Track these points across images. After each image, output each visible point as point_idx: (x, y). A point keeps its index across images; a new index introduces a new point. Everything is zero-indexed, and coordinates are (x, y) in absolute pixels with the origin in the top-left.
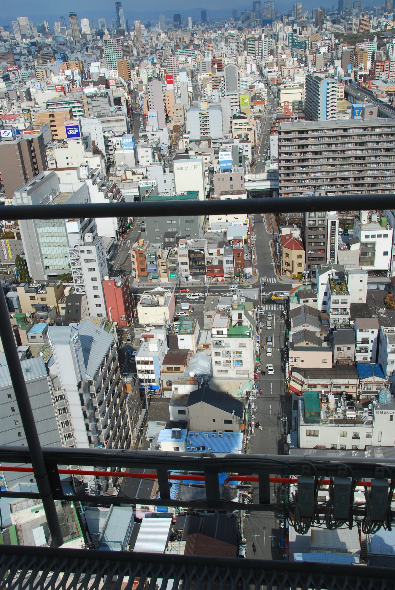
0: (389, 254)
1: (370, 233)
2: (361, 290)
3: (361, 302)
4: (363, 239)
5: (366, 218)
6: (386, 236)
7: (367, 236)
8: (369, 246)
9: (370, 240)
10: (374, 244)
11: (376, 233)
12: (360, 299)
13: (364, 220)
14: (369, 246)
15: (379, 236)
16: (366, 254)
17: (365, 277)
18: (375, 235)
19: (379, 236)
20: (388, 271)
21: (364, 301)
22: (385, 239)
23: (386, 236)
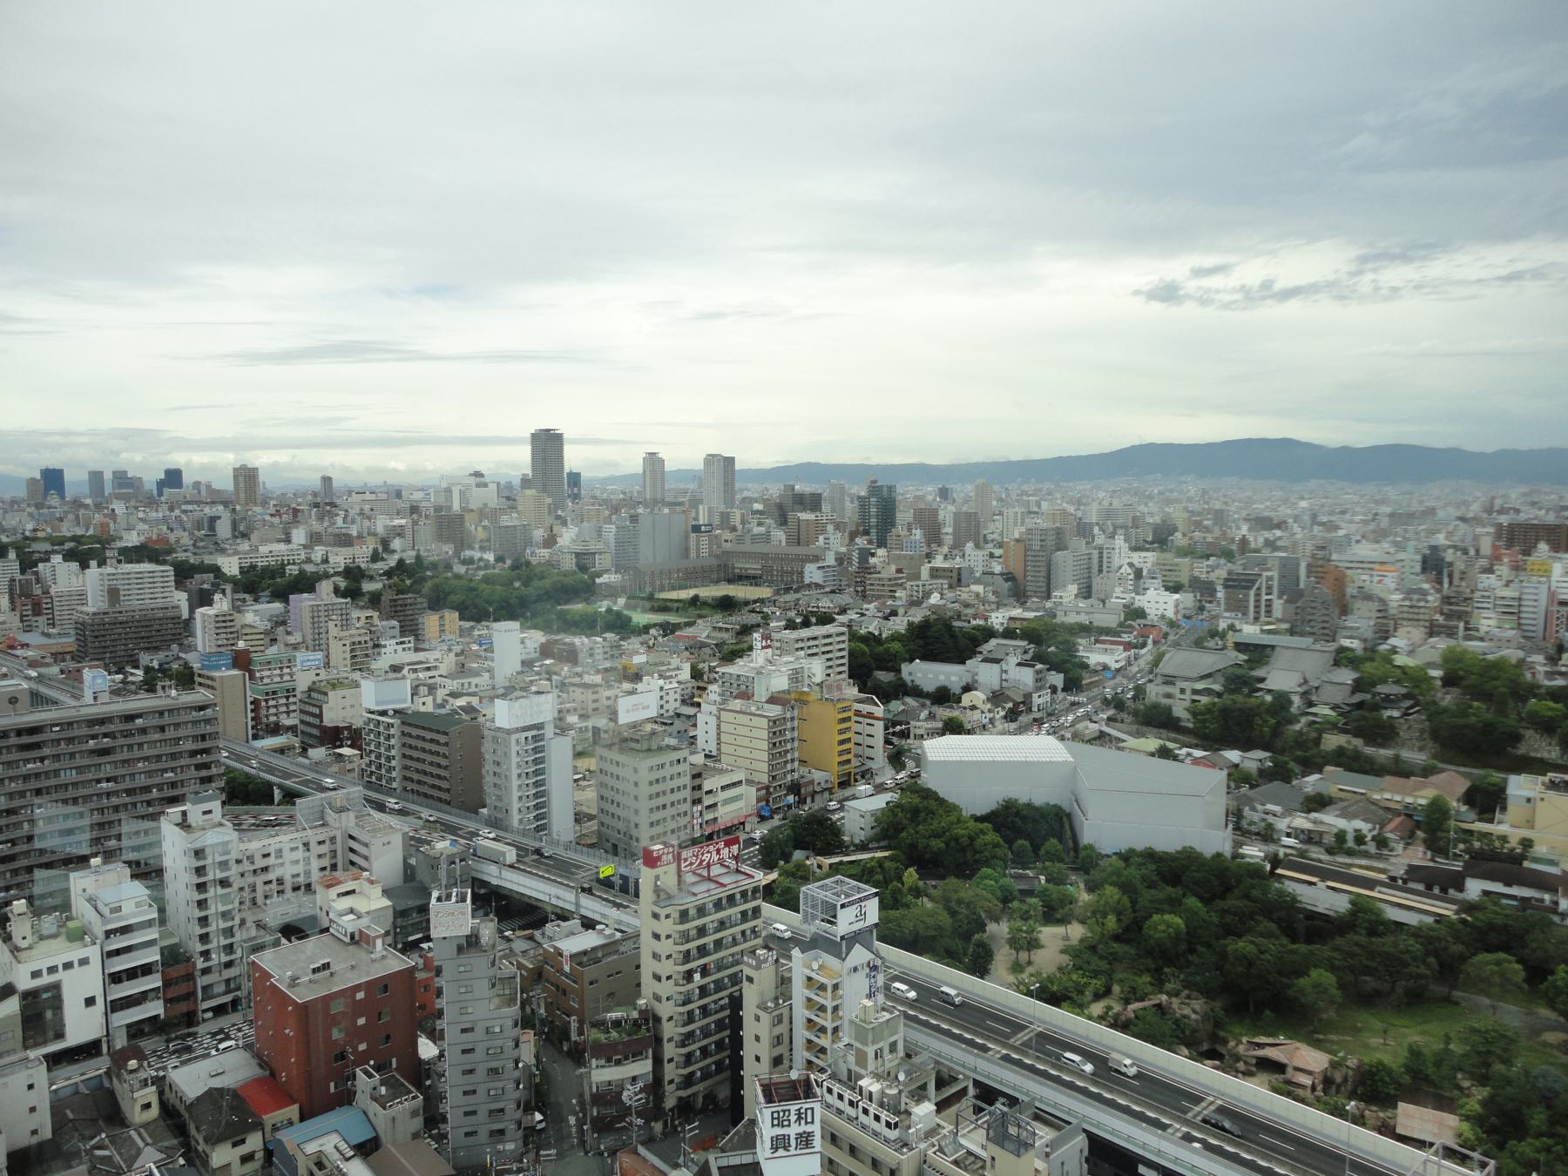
0: (100, 1001)
1: (43, 965)
2: (33, 1110)
3: (35, 1140)
4: (24, 983)
5: (28, 933)
6: (84, 962)
7: (36, 974)
8: (45, 996)
9: (46, 979)
10: (56, 987)
11: (59, 961)
12: (34, 1132)
13: (24, 938)
14: (45, 996)
15: (68, 966)
16: (40, 1016)
17: (40, 1074)
18: (56, 966)
19: (68, 966)
20: (104, 1039)
21: (47, 1133)
22: (85, 968)
23: (84, 962)
